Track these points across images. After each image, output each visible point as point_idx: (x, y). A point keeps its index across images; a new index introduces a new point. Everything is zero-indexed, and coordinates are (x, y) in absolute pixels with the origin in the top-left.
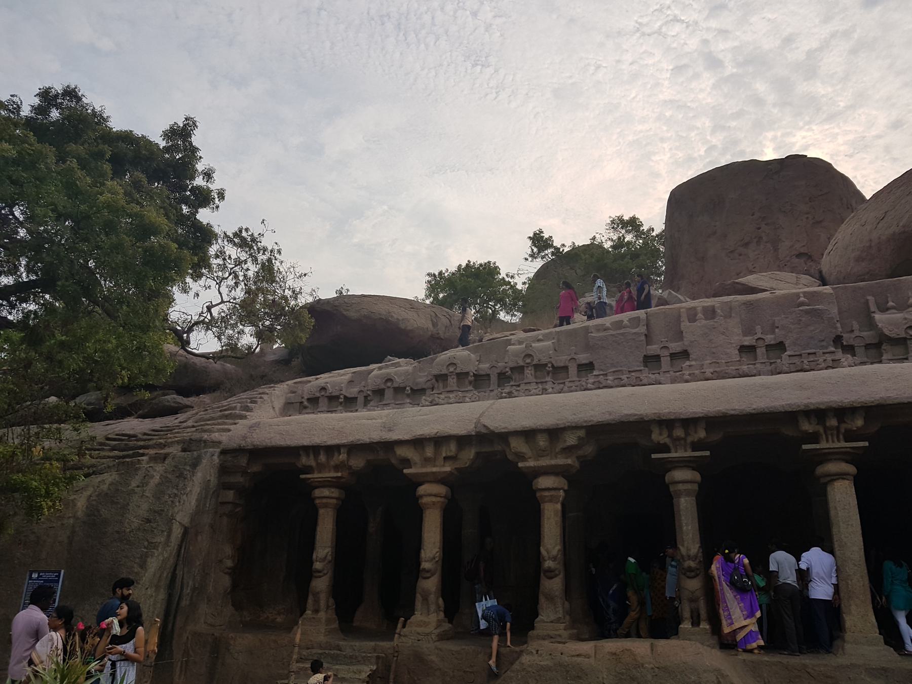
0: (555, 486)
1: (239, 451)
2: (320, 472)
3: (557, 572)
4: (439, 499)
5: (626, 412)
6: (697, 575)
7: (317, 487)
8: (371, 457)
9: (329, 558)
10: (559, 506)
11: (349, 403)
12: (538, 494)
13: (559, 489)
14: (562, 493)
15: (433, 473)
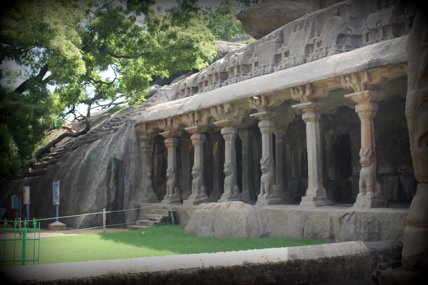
0: (226, 132)
1: (141, 124)
2: (166, 131)
3: (229, 173)
4: (197, 141)
5: (238, 95)
6: (267, 172)
7: (166, 138)
8: (179, 123)
9: (172, 170)
10: (230, 142)
11: (195, 90)
12: (224, 136)
13: (230, 133)
14: (231, 135)
15: (193, 129)
